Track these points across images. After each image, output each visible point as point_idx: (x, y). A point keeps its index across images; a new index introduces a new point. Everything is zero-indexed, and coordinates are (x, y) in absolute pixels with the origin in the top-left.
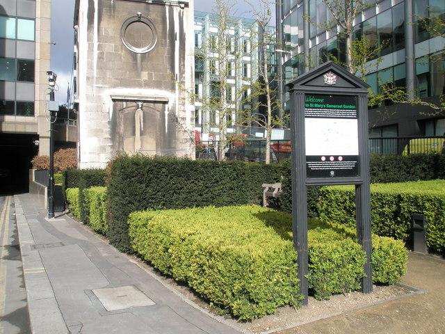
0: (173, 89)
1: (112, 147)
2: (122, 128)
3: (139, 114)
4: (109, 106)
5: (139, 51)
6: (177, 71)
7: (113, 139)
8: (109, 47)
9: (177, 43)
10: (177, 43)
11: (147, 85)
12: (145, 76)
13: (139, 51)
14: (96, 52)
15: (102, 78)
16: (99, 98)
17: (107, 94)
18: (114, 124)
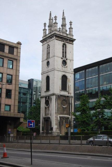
0: (70, 115)
1: (59, 128)
2: (61, 123)
3: (64, 120)
4: (59, 119)
5: (64, 107)
6: (71, 111)
7: (59, 126)
8: (59, 106)
9: (71, 105)
10: (71, 105)
11: (65, 114)
12: (65, 112)
13: (64, 107)
14: (57, 107)
15: (58, 113)
16: (57, 117)
17: (58, 116)
18: (60, 123)
